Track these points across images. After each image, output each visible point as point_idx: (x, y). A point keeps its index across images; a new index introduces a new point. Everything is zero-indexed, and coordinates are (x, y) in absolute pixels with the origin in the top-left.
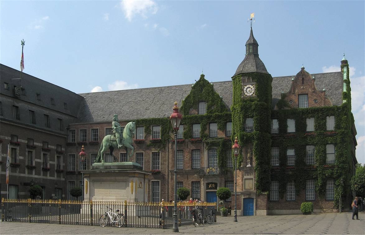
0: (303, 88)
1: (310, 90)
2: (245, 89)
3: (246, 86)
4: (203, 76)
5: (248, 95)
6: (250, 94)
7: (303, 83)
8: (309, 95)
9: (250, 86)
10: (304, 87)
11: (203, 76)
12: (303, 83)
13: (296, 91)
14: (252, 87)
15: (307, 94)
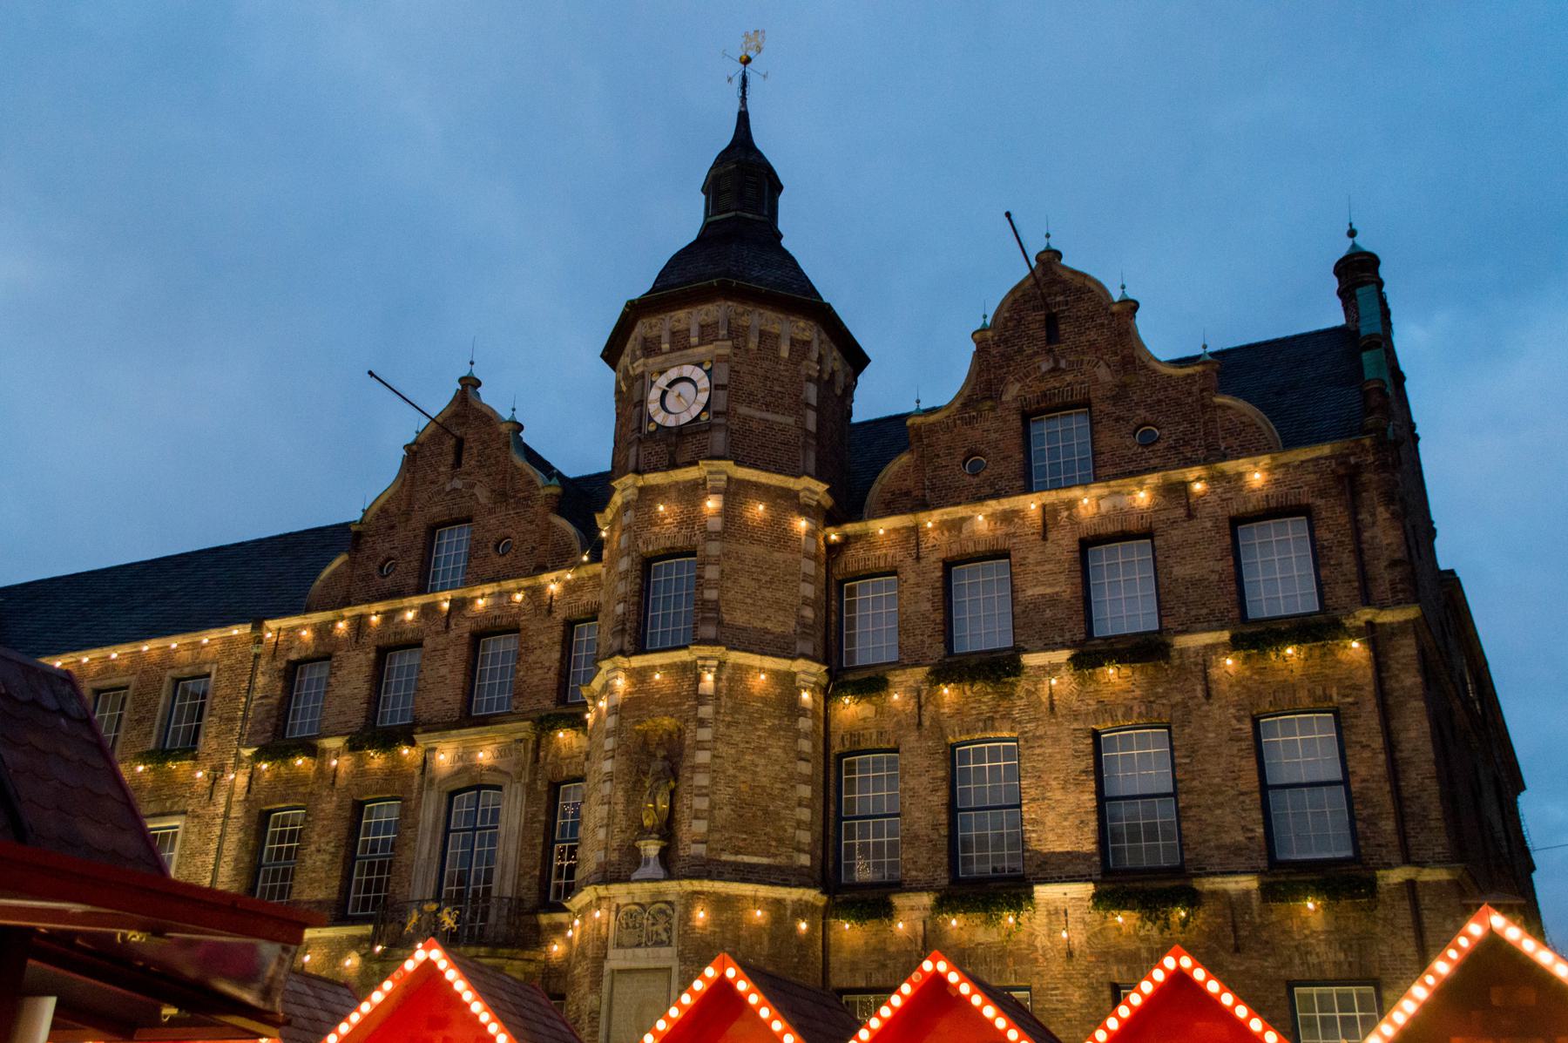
0: (1053, 370)
1: (1103, 373)
2: (654, 394)
3: (661, 373)
4: (470, 384)
5: (671, 422)
6: (685, 418)
7: (1052, 336)
8: (1098, 406)
9: (687, 371)
10: (1063, 364)
11: (470, 384)
12: (1052, 336)
13: (1012, 391)
14: (698, 374)
15: (1086, 404)
